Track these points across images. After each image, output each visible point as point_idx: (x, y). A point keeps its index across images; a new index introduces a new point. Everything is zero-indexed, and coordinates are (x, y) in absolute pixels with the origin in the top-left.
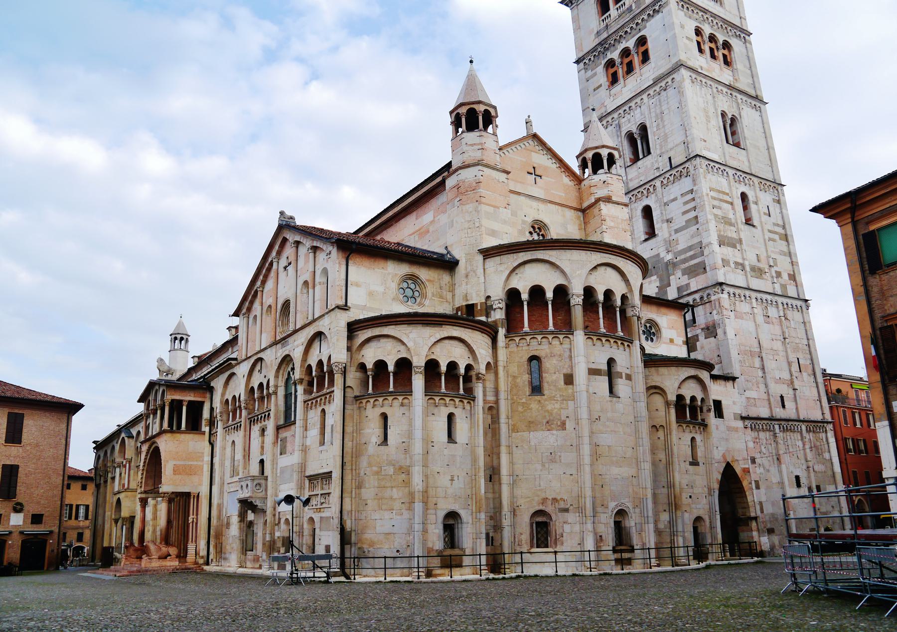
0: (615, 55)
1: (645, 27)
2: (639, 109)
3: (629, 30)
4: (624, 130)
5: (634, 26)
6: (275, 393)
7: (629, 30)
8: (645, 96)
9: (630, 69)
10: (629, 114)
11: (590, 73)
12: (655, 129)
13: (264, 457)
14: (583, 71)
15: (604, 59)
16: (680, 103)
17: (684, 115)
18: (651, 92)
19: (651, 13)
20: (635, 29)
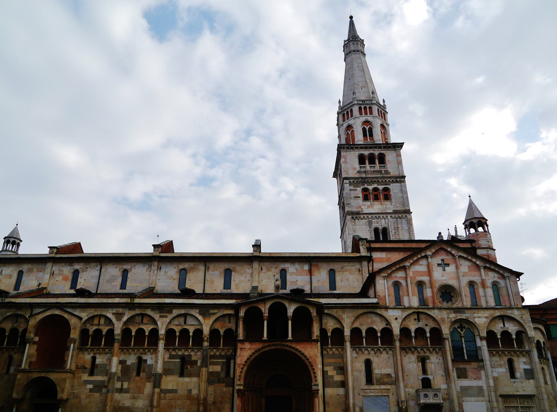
0: (371, 188)
1: (390, 185)
2: (383, 220)
3: (380, 181)
4: (374, 225)
5: (384, 181)
6: (448, 339)
7: (380, 181)
8: (389, 216)
9: (376, 198)
10: (377, 219)
11: (352, 188)
12: (393, 233)
13: (430, 377)
14: (349, 185)
15: (362, 186)
16: (409, 228)
17: (412, 235)
18: (393, 216)
19: (395, 180)
20: (384, 183)
